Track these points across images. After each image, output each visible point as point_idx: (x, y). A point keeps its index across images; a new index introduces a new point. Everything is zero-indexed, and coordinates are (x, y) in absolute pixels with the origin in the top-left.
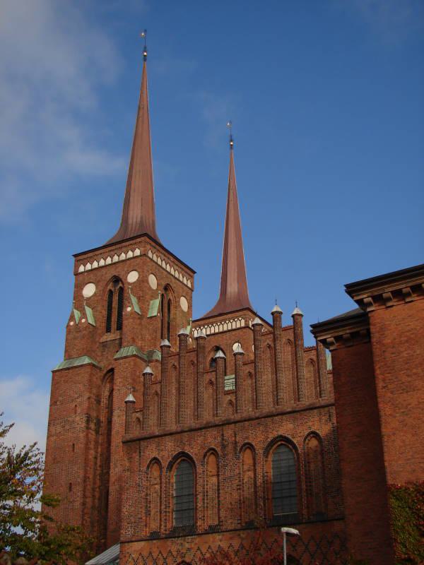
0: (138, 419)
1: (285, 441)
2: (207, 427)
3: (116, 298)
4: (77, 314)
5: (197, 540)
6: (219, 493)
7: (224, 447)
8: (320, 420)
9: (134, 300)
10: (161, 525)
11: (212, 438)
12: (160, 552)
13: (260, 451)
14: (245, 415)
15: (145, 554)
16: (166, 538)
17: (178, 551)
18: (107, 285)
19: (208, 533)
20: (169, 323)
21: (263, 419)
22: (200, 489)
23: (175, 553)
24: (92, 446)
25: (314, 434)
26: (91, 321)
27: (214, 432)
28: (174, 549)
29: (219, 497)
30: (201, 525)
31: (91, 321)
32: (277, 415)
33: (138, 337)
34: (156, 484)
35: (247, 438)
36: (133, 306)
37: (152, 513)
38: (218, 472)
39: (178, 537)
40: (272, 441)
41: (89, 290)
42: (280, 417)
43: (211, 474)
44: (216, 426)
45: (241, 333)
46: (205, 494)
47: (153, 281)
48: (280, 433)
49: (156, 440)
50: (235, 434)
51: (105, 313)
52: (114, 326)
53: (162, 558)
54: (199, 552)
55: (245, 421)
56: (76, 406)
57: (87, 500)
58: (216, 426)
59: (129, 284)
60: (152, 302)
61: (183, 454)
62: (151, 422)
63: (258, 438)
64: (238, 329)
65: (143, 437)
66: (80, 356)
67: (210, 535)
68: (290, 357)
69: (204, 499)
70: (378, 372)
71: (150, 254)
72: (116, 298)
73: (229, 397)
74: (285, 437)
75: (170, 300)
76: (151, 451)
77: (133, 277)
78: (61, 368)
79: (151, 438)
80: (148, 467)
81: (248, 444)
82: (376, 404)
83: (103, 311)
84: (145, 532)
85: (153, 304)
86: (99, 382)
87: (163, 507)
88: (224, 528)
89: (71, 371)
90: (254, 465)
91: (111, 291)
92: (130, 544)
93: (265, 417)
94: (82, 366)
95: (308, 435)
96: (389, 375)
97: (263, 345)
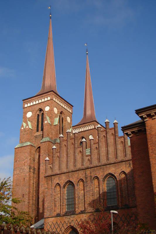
1: (112, 175)
2: (79, 170)
3: (40, 118)
4: (24, 124)
5: (76, 216)
6: (84, 197)
7: (86, 178)
8: (126, 167)
9: (48, 118)
10: (61, 211)
11: (81, 175)
12: (61, 222)
13: (101, 180)
14: (95, 165)
15: (55, 222)
16: (63, 216)
17: (68, 221)
18: (36, 112)
19: (80, 214)
20: (62, 128)
21: (102, 166)
22: (76, 196)
23: (67, 222)
24: (32, 179)
25: (124, 172)
26: (30, 127)
27: (82, 172)
28: (66, 220)
29: (84, 199)
30: (78, 210)
31: (30, 127)
32: (108, 164)
33: (50, 134)
34: (59, 194)
35: (96, 174)
36: (47, 121)
37: (57, 206)
38: (84, 188)
39: (68, 215)
40: (106, 175)
41: (29, 115)
42: (109, 165)
43: (81, 189)
44: (82, 170)
45: (93, 131)
46: (79, 197)
47: (56, 110)
49: (58, 176)
50: (91, 173)
51: (36, 124)
52: (40, 129)
53: (61, 224)
54: (77, 221)
55: (95, 167)
56: (25, 162)
57: (30, 201)
59: (46, 111)
60: (55, 119)
61: (70, 181)
62: (56, 169)
63: (101, 174)
64: (91, 129)
65: (53, 174)
66: (26, 142)
67: (81, 214)
68: (113, 140)
69: (78, 200)
70: (149, 146)
71: (54, 99)
72: (40, 118)
73: (88, 158)
74: (111, 174)
75: (63, 118)
76: (56, 180)
77: (47, 109)
78: (18, 147)
79: (56, 175)
80: (55, 187)
81: (96, 177)
82: (149, 159)
83: (35, 123)
84: (55, 214)
85: (56, 120)
86: (34, 152)
87: (62, 203)
88: (87, 212)
89: (22, 148)
90: (99, 185)
91: (38, 114)
92: (48, 219)
93: (103, 166)
94: (27, 146)
95: (121, 172)
96: (154, 147)
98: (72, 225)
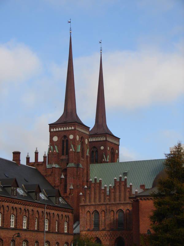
0: (84, 200)
1: (121, 210)
2: (102, 204)
5: (100, 232)
7: (106, 210)
11: (103, 208)
14: (112, 203)
22: (100, 220)
25: (128, 210)
27: (104, 206)
29: (105, 222)
30: (101, 228)
31: (57, 151)
44: (105, 205)
47: (78, 137)
48: (120, 208)
58: (105, 205)
59: (70, 139)
61: (96, 210)
63: (115, 209)
73: (108, 197)
77: (71, 137)
80: (87, 213)
84: (86, 229)
90: (114, 215)
97: (117, 185)
98: (97, 236)
